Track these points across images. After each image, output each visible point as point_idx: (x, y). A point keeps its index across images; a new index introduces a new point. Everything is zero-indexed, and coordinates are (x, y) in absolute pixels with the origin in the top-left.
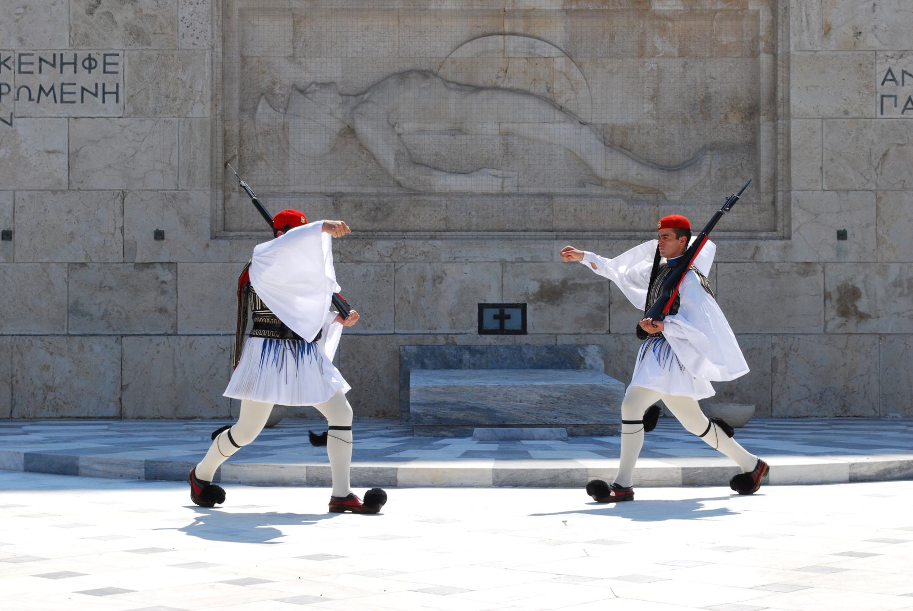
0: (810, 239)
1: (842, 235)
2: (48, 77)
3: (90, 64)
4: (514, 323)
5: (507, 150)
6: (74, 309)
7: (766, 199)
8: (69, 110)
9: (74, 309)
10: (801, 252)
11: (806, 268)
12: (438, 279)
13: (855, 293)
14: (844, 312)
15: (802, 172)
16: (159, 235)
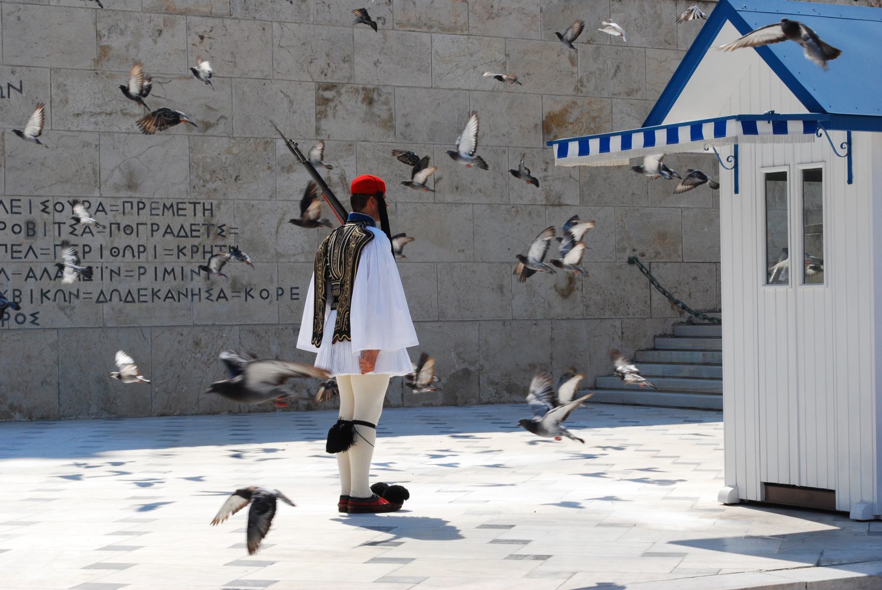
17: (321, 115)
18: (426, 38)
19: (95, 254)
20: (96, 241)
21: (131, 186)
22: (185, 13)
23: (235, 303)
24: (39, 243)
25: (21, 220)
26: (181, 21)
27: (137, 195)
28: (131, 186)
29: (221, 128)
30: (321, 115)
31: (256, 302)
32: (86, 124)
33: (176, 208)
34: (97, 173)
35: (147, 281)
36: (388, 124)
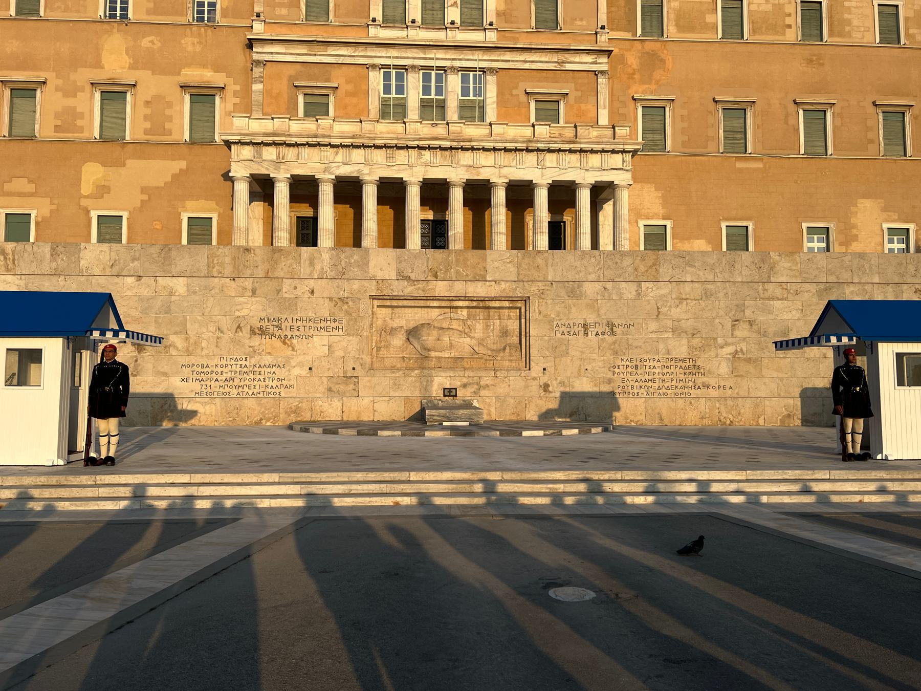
0: (536, 370)
1: (544, 369)
2: (323, 324)
3: (335, 320)
4: (453, 393)
5: (451, 345)
6: (330, 390)
7: (524, 359)
8: (329, 333)
9: (330, 390)
10: (534, 375)
11: (534, 378)
12: (432, 381)
13: (548, 386)
14: (545, 391)
15: (534, 352)
16: (354, 369)
17: (733, 330)
18: (772, 303)
19: (656, 375)
20: (657, 371)
21: (668, 352)
22: (686, 299)
23: (704, 390)
24: (639, 371)
25: (633, 364)
26: (685, 302)
27: (670, 357)
28: (668, 352)
29: (698, 335)
30: (733, 330)
31: (711, 390)
32: (654, 335)
33: (683, 360)
34: (657, 350)
35: (674, 383)
36: (759, 332)
